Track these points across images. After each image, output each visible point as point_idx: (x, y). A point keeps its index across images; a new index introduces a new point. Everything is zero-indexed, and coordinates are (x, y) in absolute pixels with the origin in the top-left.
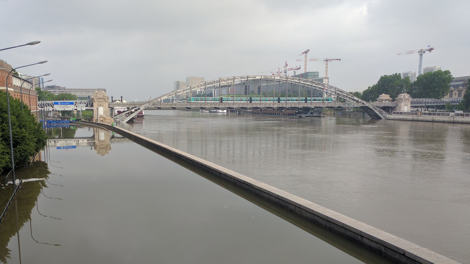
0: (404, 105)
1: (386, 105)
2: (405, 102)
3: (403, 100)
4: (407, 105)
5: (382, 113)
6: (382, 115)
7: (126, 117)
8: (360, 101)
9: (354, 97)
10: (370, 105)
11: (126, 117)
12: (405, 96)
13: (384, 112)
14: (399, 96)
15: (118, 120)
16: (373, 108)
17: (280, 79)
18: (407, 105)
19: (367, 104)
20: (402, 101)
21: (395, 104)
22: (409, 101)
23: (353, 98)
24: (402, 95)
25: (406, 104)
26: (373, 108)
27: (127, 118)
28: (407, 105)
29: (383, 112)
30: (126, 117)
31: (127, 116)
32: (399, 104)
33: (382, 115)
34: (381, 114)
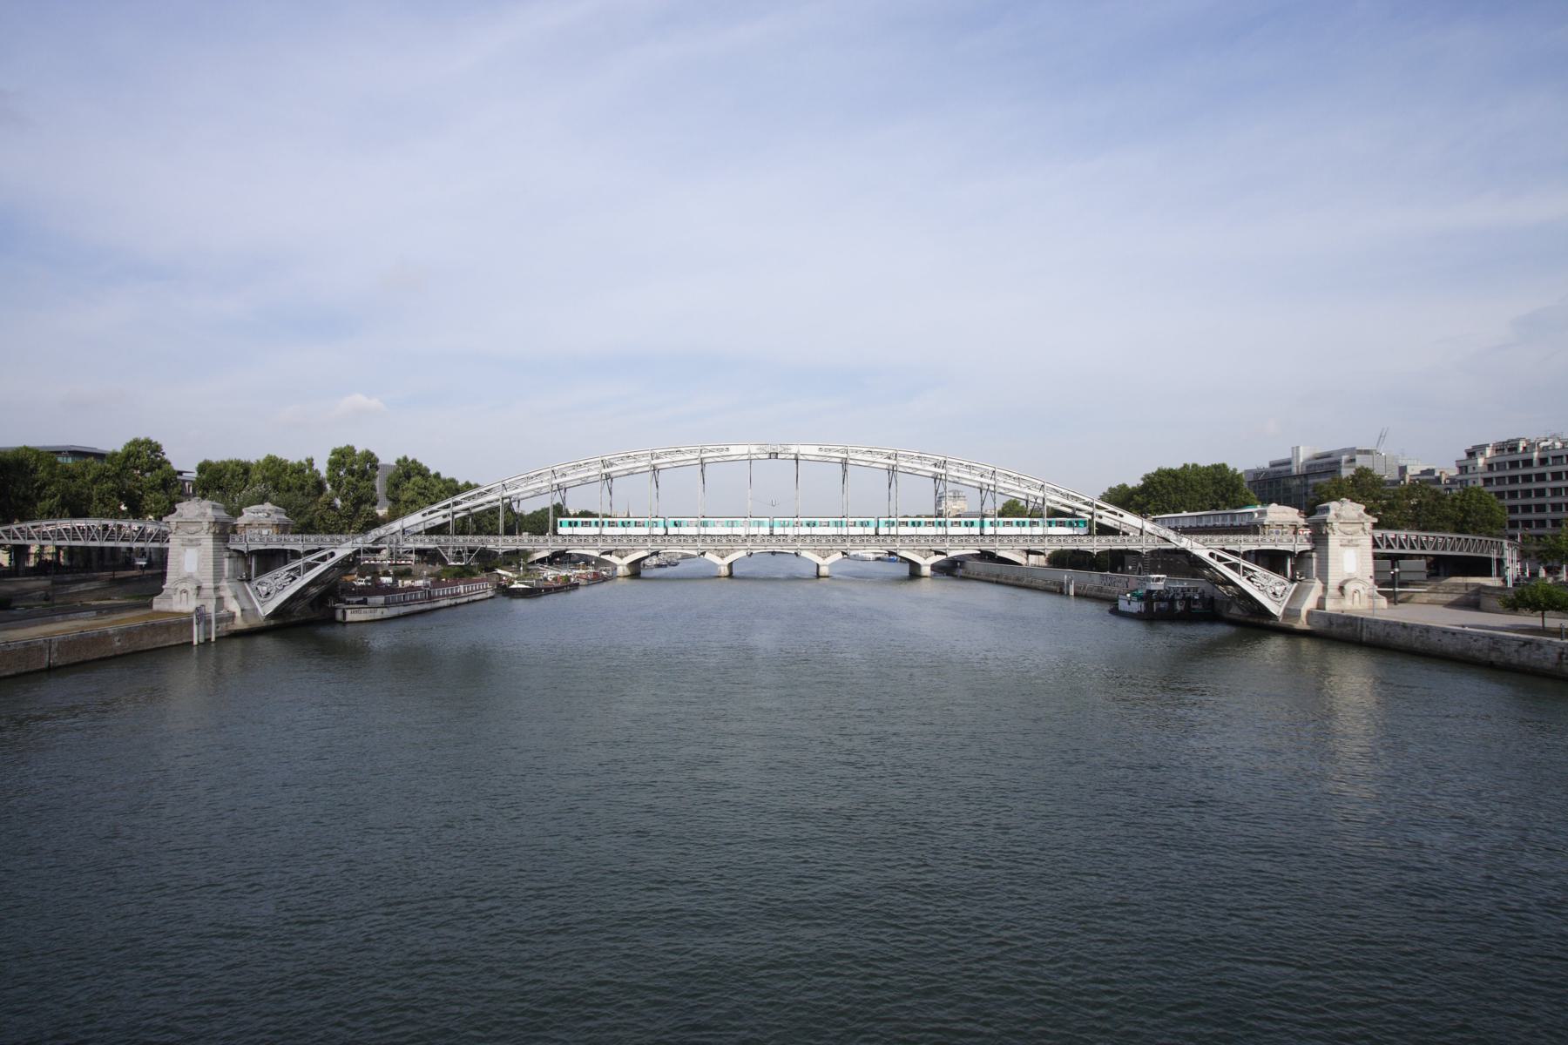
0: (1341, 545)
4: (1357, 545)
5: (1250, 574)
6: (1252, 582)
7: (290, 579)
8: (1152, 531)
9: (1121, 516)
11: (291, 581)
12: (1346, 514)
13: (1260, 571)
15: (265, 588)
17: (823, 453)
27: (294, 582)
30: (291, 581)
31: (294, 579)
33: (1250, 583)
34: (1249, 579)
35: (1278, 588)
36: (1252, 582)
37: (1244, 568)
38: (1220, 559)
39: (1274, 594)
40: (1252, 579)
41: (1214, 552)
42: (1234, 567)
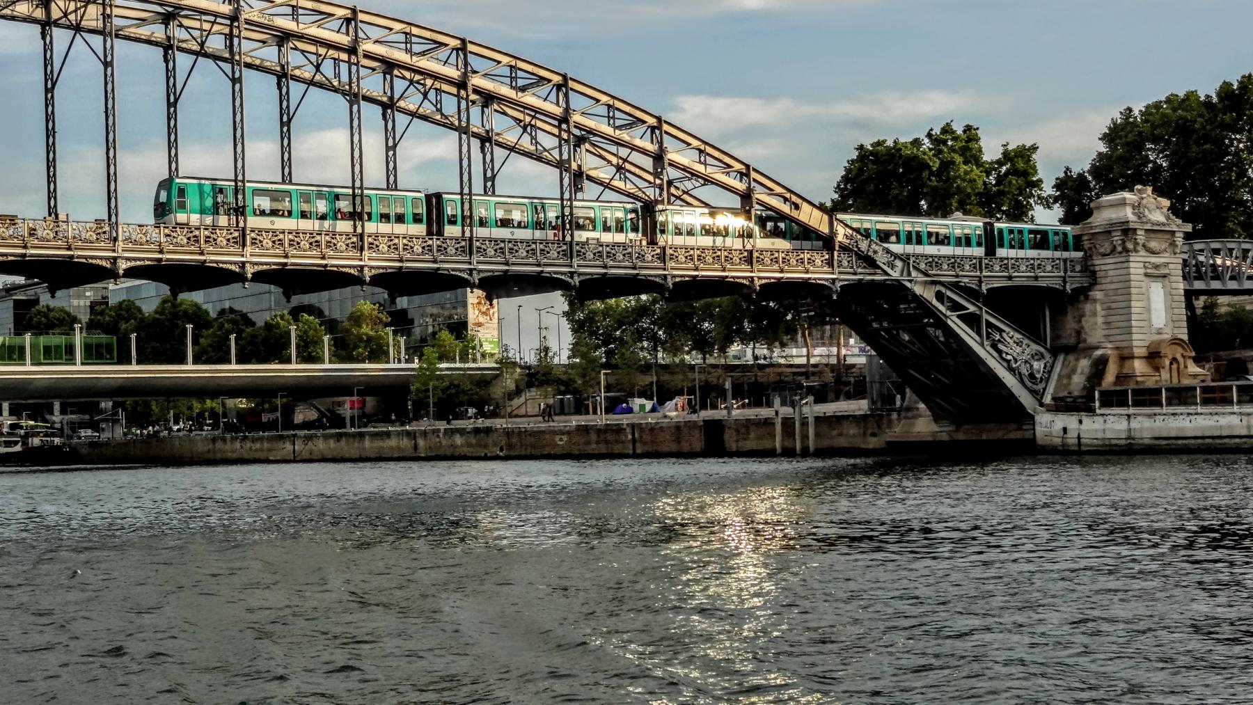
0: (1146, 275)
1: (1022, 277)
2: (1153, 252)
3: (1141, 235)
5: (998, 337)
6: (1000, 352)
9: (797, 207)
10: (914, 273)
14: (1095, 214)
16: (935, 302)
18: (1164, 271)
19: (893, 267)
20: (1130, 246)
21: (1078, 268)
22: (1173, 244)
23: (794, 214)
24: (1123, 203)
25: (1157, 267)
26: (935, 302)
28: (1164, 276)
29: (1001, 331)
32: (1104, 265)
34: (994, 346)
35: (1036, 365)
36: (1000, 352)
37: (989, 324)
38: (955, 307)
39: (1032, 376)
40: (1000, 346)
41: (943, 290)
42: (972, 321)
